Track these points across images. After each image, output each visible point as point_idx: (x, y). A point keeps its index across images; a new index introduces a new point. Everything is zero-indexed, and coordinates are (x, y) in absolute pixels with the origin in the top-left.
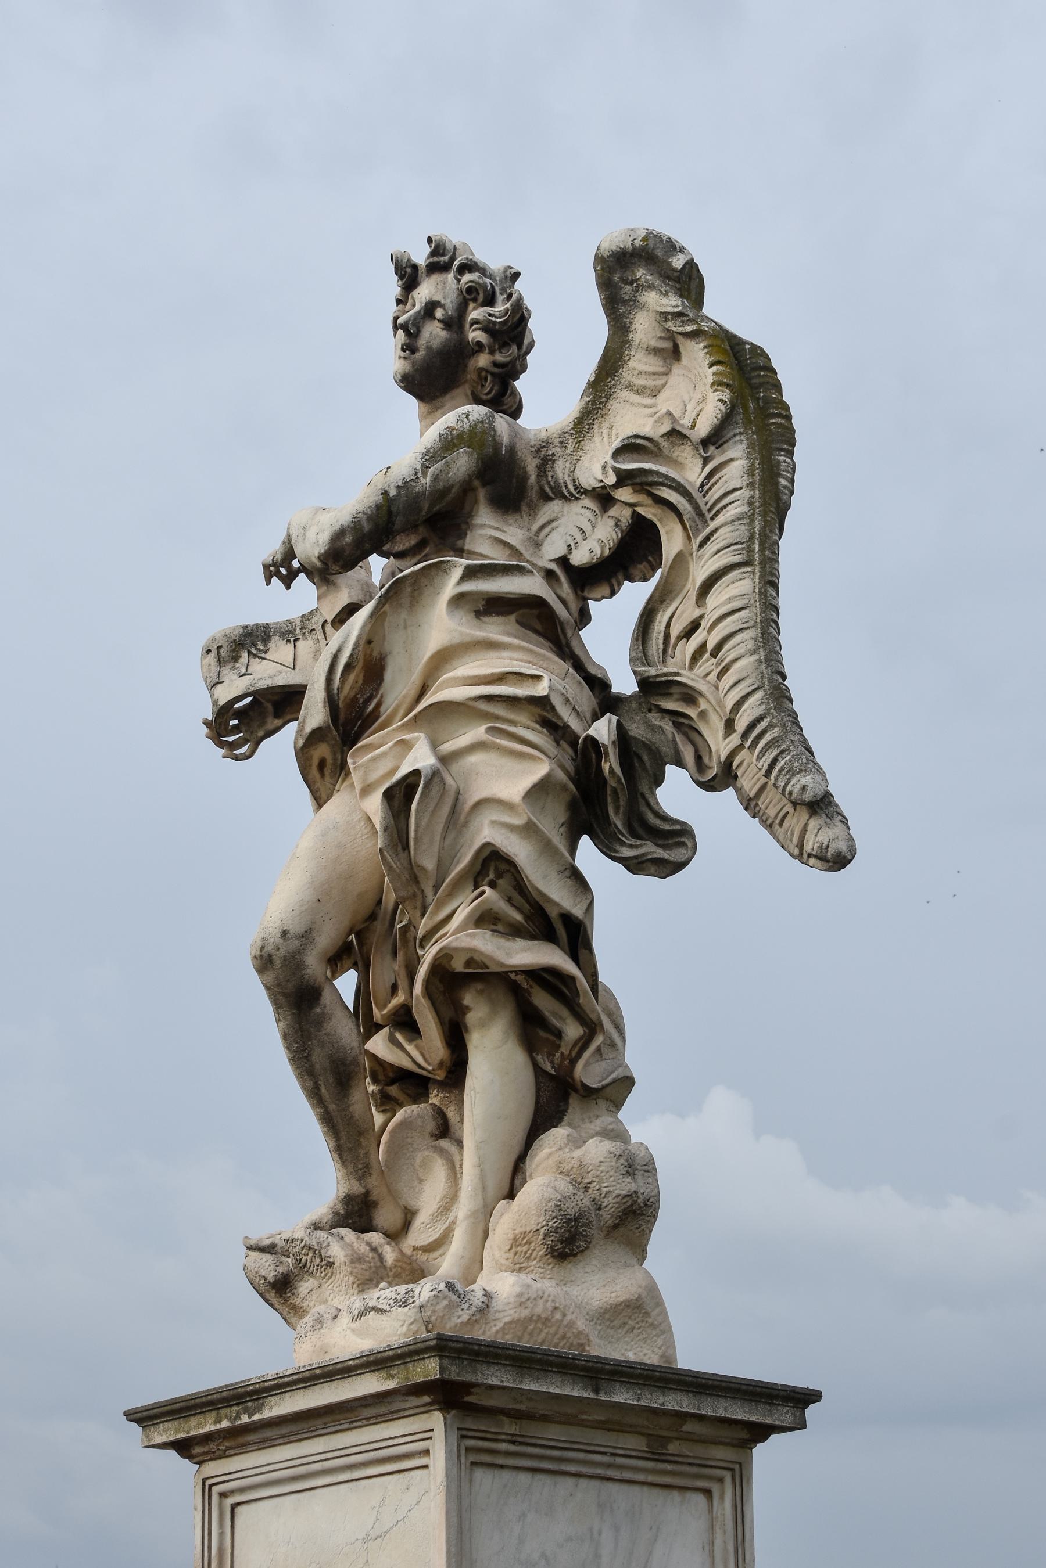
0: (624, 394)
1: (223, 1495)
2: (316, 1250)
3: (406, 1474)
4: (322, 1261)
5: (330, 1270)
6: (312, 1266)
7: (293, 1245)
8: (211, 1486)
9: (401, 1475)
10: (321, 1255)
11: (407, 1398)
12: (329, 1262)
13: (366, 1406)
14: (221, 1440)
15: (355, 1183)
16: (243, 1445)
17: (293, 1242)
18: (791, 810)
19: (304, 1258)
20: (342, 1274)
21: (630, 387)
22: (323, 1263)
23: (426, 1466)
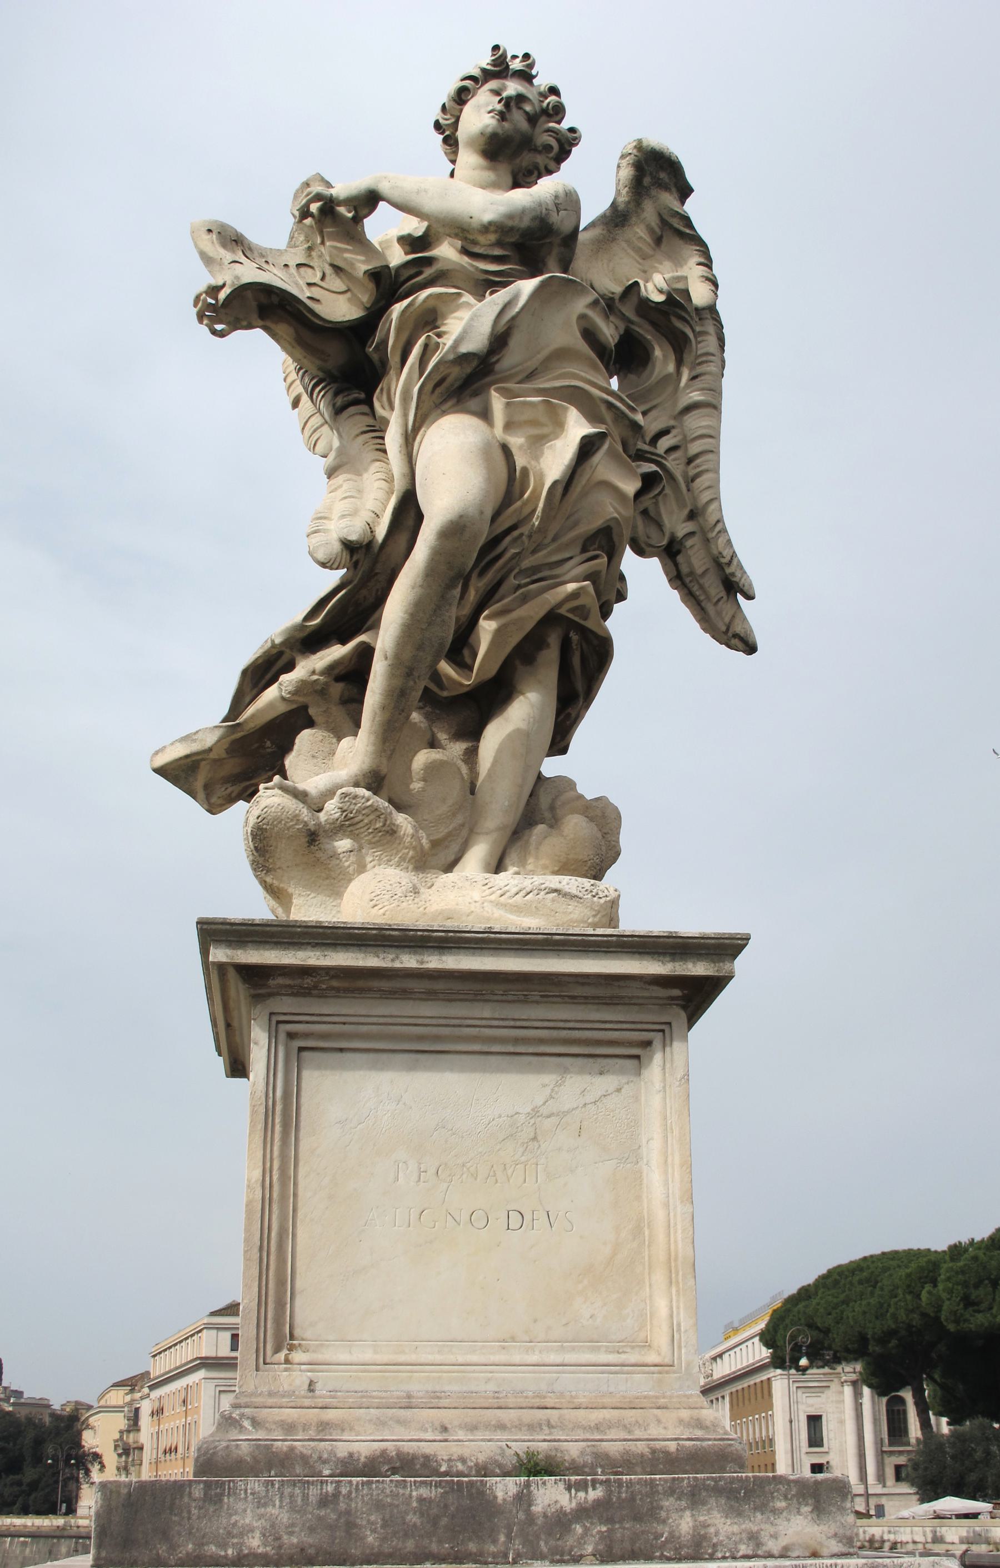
0: (624, 245)
1: (291, 1036)
2: (382, 814)
3: (599, 1060)
4: (384, 825)
5: (389, 838)
6: (366, 828)
7: (354, 801)
8: (278, 1022)
9: (591, 1060)
10: (386, 820)
11: (648, 987)
12: (392, 829)
13: (583, 984)
14: (327, 978)
15: (385, 761)
16: (361, 990)
17: (354, 799)
18: (725, 598)
19: (360, 817)
20: (402, 846)
21: (628, 242)
22: (384, 829)
23: (638, 1057)
